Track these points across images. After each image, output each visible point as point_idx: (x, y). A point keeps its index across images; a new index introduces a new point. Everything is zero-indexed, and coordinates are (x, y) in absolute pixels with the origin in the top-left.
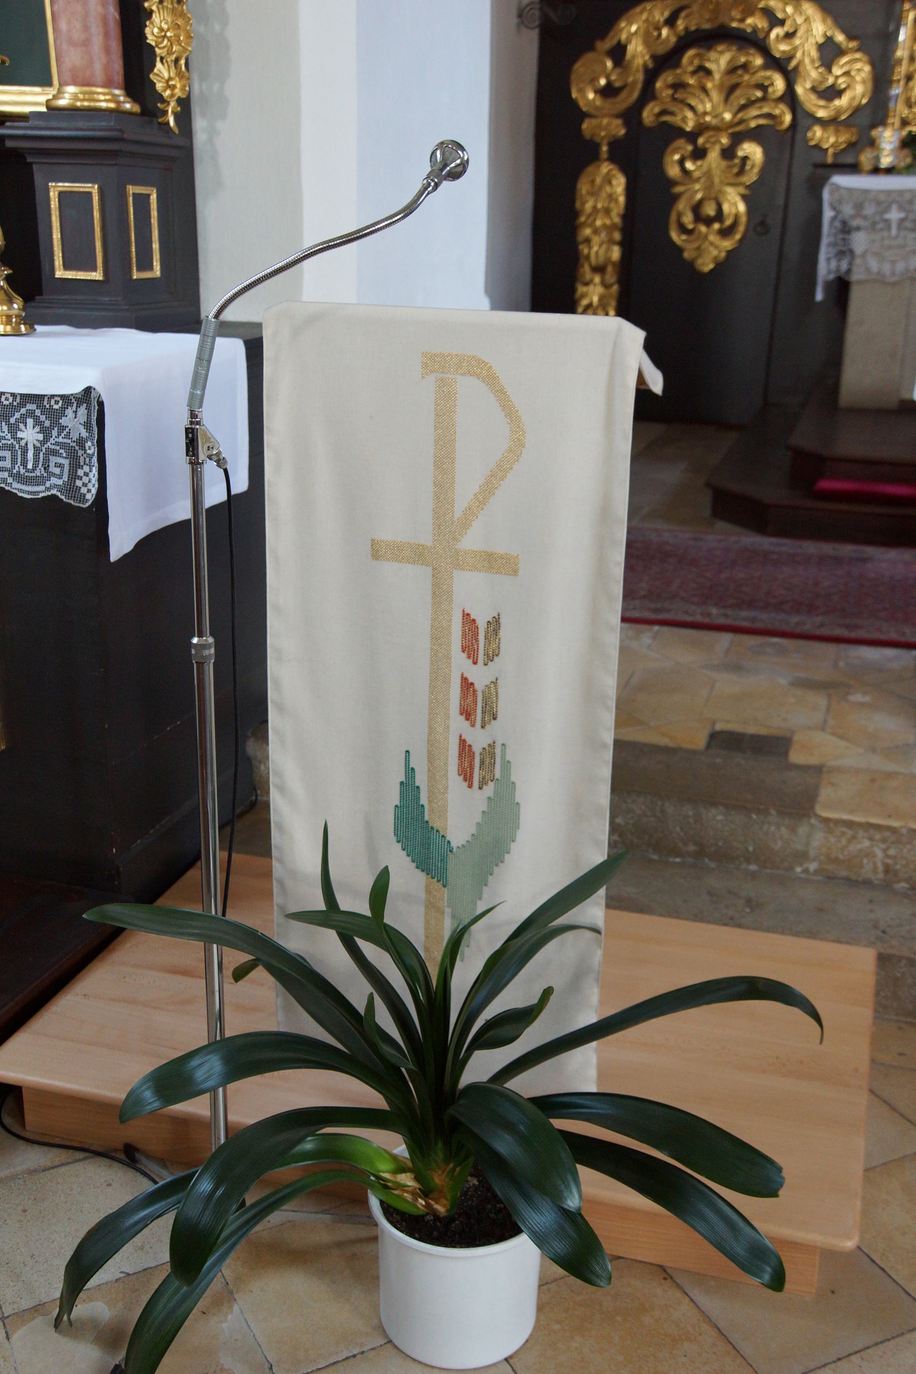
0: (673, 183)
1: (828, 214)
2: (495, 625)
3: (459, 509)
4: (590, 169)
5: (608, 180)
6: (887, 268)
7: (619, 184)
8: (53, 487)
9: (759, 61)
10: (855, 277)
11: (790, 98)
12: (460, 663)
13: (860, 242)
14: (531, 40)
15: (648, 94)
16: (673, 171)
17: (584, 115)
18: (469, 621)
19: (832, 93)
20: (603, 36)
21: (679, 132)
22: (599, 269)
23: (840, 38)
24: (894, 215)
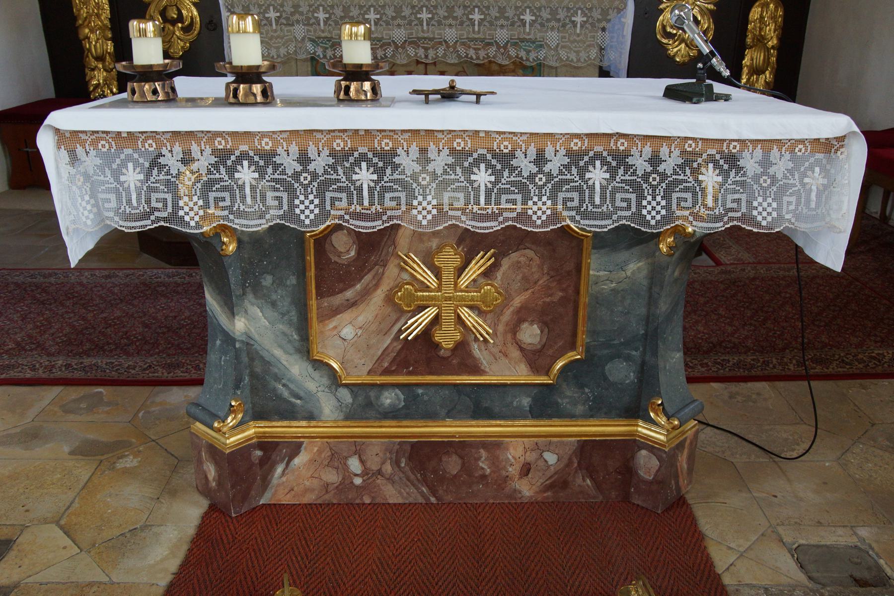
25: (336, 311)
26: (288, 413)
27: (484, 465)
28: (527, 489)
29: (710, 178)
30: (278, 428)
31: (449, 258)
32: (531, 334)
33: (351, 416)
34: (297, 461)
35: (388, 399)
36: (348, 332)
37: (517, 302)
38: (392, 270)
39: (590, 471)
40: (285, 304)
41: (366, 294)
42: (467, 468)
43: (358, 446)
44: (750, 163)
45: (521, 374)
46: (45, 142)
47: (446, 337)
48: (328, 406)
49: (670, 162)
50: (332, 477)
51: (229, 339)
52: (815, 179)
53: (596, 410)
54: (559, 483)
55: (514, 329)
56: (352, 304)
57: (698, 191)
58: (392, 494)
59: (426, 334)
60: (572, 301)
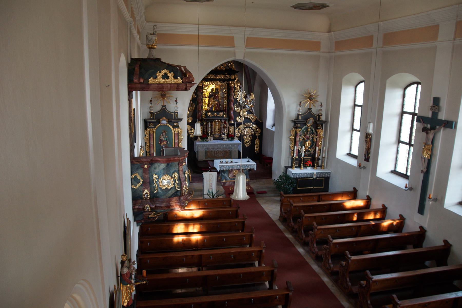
2: (212, 183)
3: (211, 178)
6: (202, 150)
10: (199, 151)
12: (210, 185)
13: (199, 148)
18: (211, 183)
26: (227, 180)
29: (249, 166)
30: (226, 181)
31: (236, 171)
33: (230, 180)
34: (228, 183)
35: (233, 179)
38: (233, 172)
43: (231, 182)
44: (251, 165)
48: (229, 180)
49: (247, 165)
50: (229, 184)
51: (224, 176)
52: (254, 166)
57: (249, 167)
59: (235, 175)
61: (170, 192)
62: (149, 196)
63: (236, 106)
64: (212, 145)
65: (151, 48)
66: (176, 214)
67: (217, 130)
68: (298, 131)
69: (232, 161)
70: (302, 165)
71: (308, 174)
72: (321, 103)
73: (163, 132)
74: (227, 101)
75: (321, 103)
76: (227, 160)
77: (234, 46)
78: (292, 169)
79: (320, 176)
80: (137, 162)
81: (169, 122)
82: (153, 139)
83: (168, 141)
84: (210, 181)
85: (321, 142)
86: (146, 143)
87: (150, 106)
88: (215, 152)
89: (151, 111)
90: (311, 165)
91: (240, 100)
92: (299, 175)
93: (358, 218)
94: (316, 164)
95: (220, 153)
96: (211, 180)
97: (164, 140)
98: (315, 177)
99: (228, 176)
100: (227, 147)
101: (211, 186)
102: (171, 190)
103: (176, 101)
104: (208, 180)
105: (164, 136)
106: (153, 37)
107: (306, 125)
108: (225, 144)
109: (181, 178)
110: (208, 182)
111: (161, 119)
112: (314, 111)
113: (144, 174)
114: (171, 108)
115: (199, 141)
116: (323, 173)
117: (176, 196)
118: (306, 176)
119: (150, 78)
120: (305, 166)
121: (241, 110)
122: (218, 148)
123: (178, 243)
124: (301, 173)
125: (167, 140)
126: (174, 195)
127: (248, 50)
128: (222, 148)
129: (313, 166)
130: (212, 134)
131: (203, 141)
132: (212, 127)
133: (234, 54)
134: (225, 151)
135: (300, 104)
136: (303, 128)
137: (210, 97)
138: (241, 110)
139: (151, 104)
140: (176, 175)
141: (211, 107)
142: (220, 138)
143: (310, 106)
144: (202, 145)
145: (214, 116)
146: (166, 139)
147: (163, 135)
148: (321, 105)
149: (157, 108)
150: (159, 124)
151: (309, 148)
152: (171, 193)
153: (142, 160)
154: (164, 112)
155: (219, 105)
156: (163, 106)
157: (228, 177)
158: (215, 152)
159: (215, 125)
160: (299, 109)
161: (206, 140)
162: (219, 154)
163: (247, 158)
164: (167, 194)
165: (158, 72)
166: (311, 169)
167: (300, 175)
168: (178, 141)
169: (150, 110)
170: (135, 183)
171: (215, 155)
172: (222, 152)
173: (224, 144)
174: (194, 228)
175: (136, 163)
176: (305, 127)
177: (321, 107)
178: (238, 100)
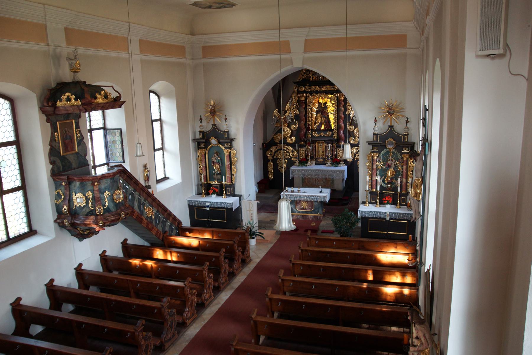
0: (278, 164)
1: (290, 171)
3: (251, 208)
4: (269, 162)
5: (271, 163)
7: (272, 163)
8: (230, 207)
9: (286, 152)
11: (289, 155)
14: (262, 151)
15: (275, 155)
16: (278, 163)
17: (268, 157)
19: (293, 155)
20: (269, 149)
21: (278, 159)
22: (271, 173)
23: (294, 150)
24: (297, 171)
25: (297, 205)
26: (294, 213)
27: (307, 217)
28: (310, 219)
31: (305, 202)
32: (310, 208)
34: (294, 216)
35: (301, 212)
36: (298, 207)
37: (309, 205)
39: (315, 218)
40: (294, 205)
41: (299, 204)
42: (306, 217)
43: (298, 215)
45: (309, 211)
46: (281, 195)
47: (304, 208)
48: (296, 212)
49: (316, 197)
50: (297, 218)
53: (315, 213)
54: (312, 219)
55: (309, 207)
56: (298, 205)
58: (301, 219)
60: (313, 205)
61: (84, 210)
62: (68, 212)
63: (349, 124)
64: (309, 170)
65: (75, 71)
66: (174, 240)
67: (321, 153)
68: (374, 156)
69: (299, 190)
70: (378, 201)
71: (381, 213)
72: (408, 119)
73: (215, 153)
74: (337, 118)
75: (408, 119)
76: (292, 189)
77: (290, 52)
78: (365, 205)
79: (400, 218)
80: (58, 179)
81: (219, 143)
82: (204, 160)
83: (220, 163)
84: (250, 211)
85: (412, 171)
86: (199, 164)
87: (200, 125)
88: (314, 180)
89: (201, 130)
90: (389, 202)
91: (353, 117)
92: (368, 214)
93: (374, 277)
94: (398, 202)
95: (320, 181)
96: (251, 210)
97: (216, 162)
98: (388, 219)
99: (295, 208)
100: (327, 174)
101: (252, 217)
102: (85, 208)
103: (226, 119)
104: (248, 209)
105: (215, 158)
106: (72, 62)
107: (387, 148)
108: (325, 171)
109: (95, 197)
110: (248, 212)
111: (210, 139)
112: (399, 128)
113: (66, 191)
114: (223, 127)
115: (296, 165)
116: (396, 213)
117: (92, 215)
118: (378, 216)
119: (57, 101)
120: (381, 203)
121: (355, 128)
122: (309, 175)
123: (136, 266)
124: (372, 212)
125: (219, 162)
126: (90, 213)
127: (308, 55)
128: (320, 174)
129: (394, 203)
130: (315, 157)
131: (302, 166)
132: (315, 149)
133: (291, 61)
134: (326, 179)
135: (376, 121)
136: (383, 152)
137: (317, 112)
138: (355, 128)
139: (201, 122)
140: (90, 194)
141: (319, 125)
142: (324, 163)
143: (391, 123)
144: (298, 170)
145: (321, 136)
146: (217, 161)
147: (215, 157)
148: (406, 121)
149: (208, 127)
150: (211, 144)
151: (392, 179)
152: (86, 211)
153: (61, 177)
154: (216, 132)
155: (328, 123)
156: (213, 125)
157: (295, 209)
158: (314, 180)
159: (318, 148)
160: (375, 127)
161: (306, 164)
162: (319, 182)
163: (320, 188)
164: (82, 212)
165: (63, 95)
166: (391, 207)
167: (371, 214)
168: (229, 163)
169: (200, 129)
170: (58, 199)
171: (314, 182)
172: (322, 180)
173: (323, 170)
174: (171, 256)
175: (57, 180)
176: (385, 151)
177: (407, 124)
178: (351, 116)
